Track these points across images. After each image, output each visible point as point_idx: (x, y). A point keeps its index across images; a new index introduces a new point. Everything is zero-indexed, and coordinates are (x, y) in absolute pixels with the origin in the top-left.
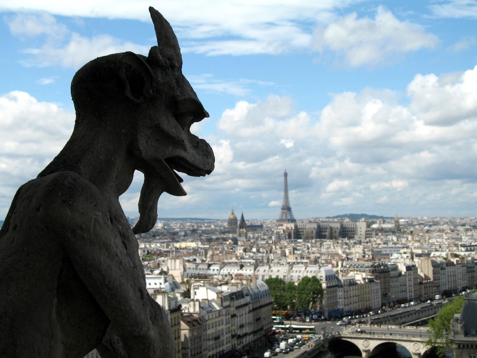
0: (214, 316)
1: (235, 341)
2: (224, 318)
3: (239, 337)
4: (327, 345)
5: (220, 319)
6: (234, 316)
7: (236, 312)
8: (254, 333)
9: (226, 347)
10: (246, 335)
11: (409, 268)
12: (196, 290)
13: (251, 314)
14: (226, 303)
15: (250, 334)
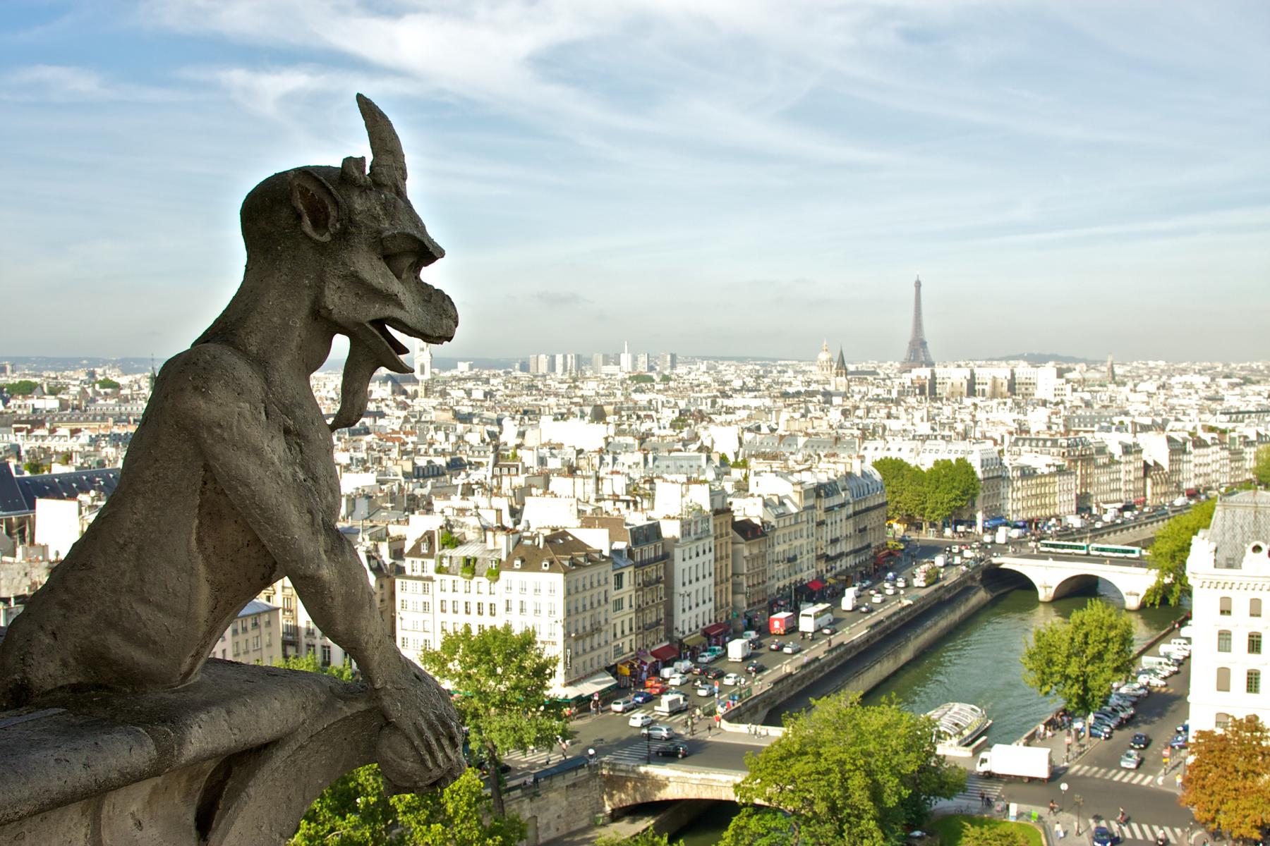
0: (787, 523)
1: (822, 566)
2: (804, 527)
3: (828, 559)
4: (978, 578)
5: (798, 527)
6: (821, 524)
7: (824, 517)
8: (856, 552)
9: (808, 575)
10: (840, 556)
11: (1127, 450)
12: (758, 478)
13: (851, 521)
14: (811, 502)
15: (848, 554)
